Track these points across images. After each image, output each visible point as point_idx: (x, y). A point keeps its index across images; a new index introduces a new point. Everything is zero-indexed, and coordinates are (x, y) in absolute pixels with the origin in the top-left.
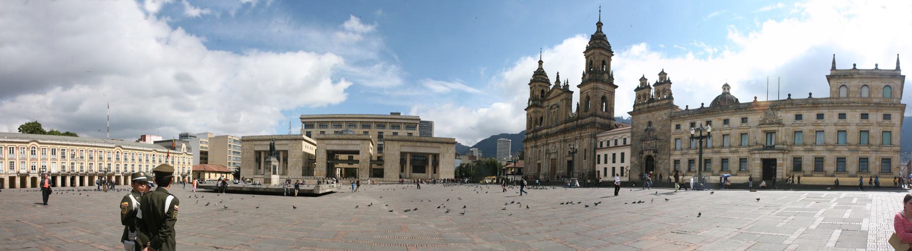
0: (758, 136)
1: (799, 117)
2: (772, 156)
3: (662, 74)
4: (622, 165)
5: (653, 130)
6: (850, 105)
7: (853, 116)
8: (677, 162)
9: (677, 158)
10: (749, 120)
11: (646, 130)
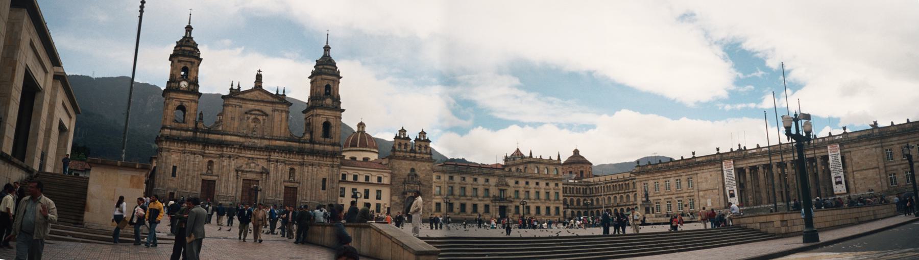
0: (494, 191)
1: (517, 183)
3: (423, 133)
4: (378, 201)
5: (416, 175)
6: (542, 179)
7: (542, 184)
8: (438, 205)
9: (438, 201)
11: (409, 175)
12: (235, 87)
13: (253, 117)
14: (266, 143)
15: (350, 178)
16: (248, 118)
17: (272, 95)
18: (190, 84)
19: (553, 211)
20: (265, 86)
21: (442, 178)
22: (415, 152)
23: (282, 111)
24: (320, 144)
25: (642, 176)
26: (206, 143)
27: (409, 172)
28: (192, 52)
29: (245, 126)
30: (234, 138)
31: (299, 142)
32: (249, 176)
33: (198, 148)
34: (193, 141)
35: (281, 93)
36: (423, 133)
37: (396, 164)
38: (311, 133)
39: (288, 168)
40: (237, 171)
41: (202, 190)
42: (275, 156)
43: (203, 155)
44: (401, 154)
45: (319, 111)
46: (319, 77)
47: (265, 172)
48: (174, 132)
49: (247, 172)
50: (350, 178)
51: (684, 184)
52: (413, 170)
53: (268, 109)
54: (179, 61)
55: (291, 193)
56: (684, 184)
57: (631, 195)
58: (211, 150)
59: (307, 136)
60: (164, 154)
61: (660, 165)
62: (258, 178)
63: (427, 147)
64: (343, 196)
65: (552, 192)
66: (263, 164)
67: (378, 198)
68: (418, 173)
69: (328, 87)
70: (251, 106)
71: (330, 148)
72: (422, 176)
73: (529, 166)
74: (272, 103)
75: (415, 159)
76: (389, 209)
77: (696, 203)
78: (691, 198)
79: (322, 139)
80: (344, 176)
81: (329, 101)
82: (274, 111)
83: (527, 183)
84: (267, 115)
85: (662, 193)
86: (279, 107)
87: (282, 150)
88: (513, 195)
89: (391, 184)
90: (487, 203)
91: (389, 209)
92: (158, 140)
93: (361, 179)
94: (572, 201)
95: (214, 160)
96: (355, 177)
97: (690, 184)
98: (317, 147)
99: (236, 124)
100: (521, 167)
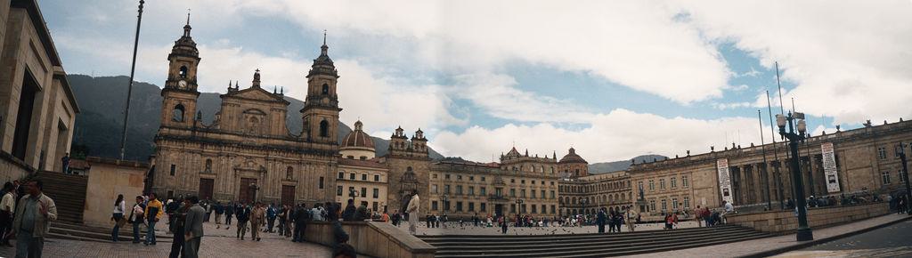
0: (490, 190)
1: (513, 181)
2: (502, 203)
3: (419, 132)
4: (376, 200)
5: (413, 174)
6: (537, 177)
8: (435, 203)
9: (435, 200)
10: (486, 180)
11: (406, 174)
12: (233, 86)
13: (251, 116)
14: (264, 142)
15: (347, 177)
16: (247, 117)
17: (269, 94)
18: (188, 83)
19: (548, 209)
20: (263, 86)
21: (439, 177)
22: (412, 151)
23: (280, 110)
24: (317, 143)
25: (637, 175)
26: (205, 142)
27: (405, 170)
28: (191, 52)
29: (243, 125)
30: (232, 137)
31: (297, 141)
32: (247, 175)
33: (196, 147)
34: (191, 140)
35: (278, 92)
36: (419, 132)
37: (393, 162)
38: (309, 132)
39: (285, 166)
40: (235, 170)
41: (200, 188)
42: (272, 155)
43: (202, 153)
44: (398, 153)
45: (317, 111)
46: (317, 77)
47: (263, 171)
48: (173, 131)
49: (245, 170)
50: (347, 177)
51: (679, 182)
52: (410, 168)
53: (266, 108)
54: (178, 61)
55: (289, 191)
56: (679, 182)
57: (626, 194)
58: (210, 149)
59: (305, 135)
60: (163, 153)
61: (655, 164)
62: (256, 176)
63: (423, 146)
64: (340, 194)
65: (548, 191)
66: (261, 162)
67: (375, 196)
68: (415, 172)
69: (325, 86)
70: (249, 105)
71: (327, 147)
72: (419, 175)
73: (525, 164)
74: (270, 102)
75: (411, 158)
76: (386, 207)
77: (691, 202)
78: (686, 197)
79: (319, 138)
80: (341, 175)
81: (326, 100)
82: (272, 110)
83: (523, 182)
84: (265, 114)
85: (657, 191)
86: (277, 106)
87: (280, 149)
88: (509, 194)
89: (388, 183)
90: (483, 201)
91: (386, 207)
92: (157, 139)
93: (359, 177)
94: (567, 199)
95: (213, 159)
96: (353, 176)
98: (314, 145)
99: (234, 123)
100: (517, 166)
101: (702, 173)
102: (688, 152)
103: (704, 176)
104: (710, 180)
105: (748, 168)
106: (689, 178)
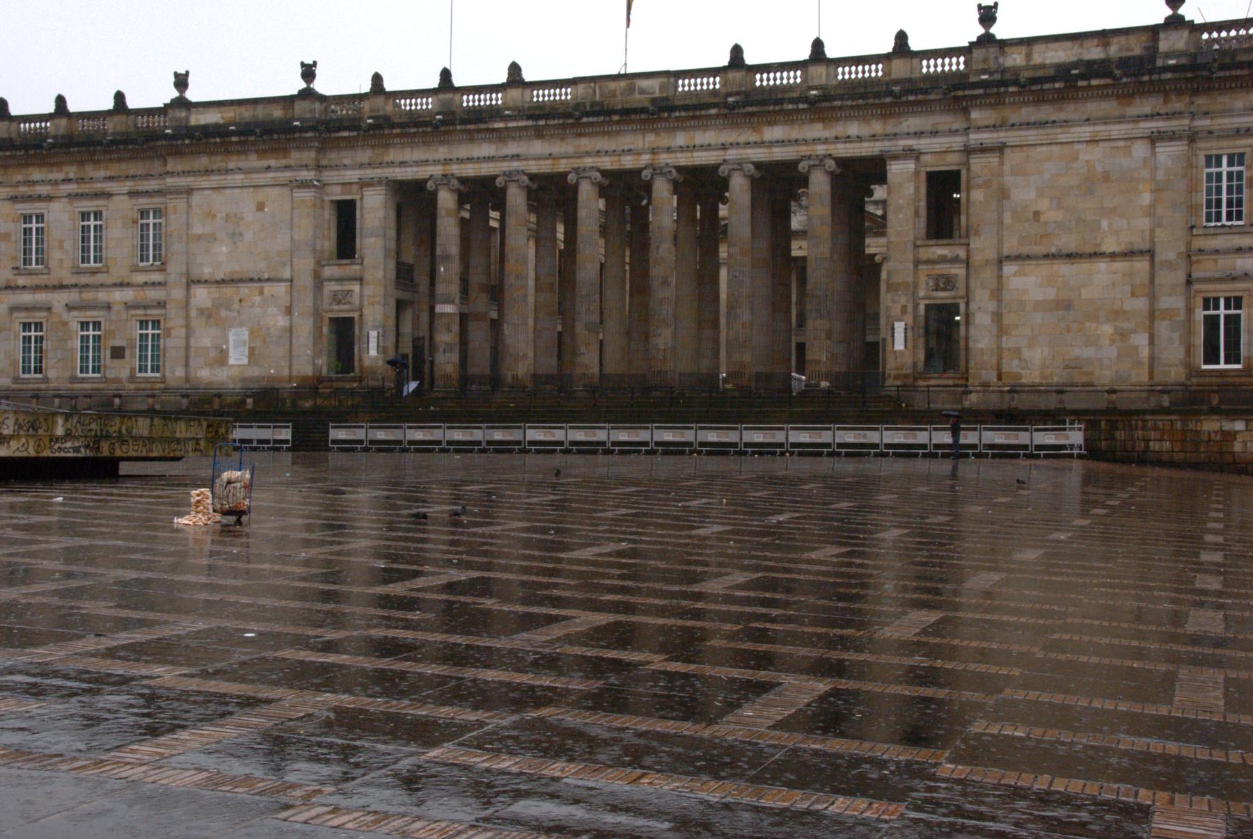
51: (119, 240)
56: (119, 240)
77: (173, 344)
78: (152, 318)
97: (153, 251)
101: (245, 202)
102: (181, 81)
103: (249, 213)
104: (282, 241)
105: (482, 194)
106: (175, 221)
